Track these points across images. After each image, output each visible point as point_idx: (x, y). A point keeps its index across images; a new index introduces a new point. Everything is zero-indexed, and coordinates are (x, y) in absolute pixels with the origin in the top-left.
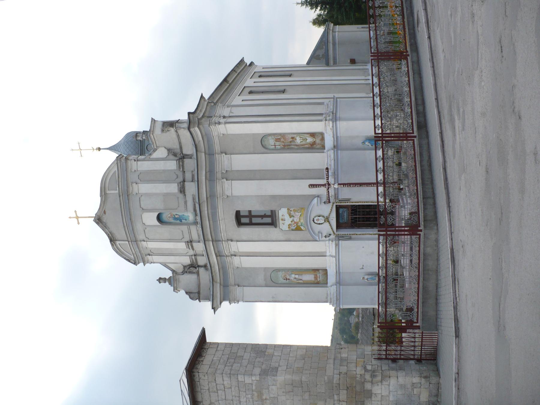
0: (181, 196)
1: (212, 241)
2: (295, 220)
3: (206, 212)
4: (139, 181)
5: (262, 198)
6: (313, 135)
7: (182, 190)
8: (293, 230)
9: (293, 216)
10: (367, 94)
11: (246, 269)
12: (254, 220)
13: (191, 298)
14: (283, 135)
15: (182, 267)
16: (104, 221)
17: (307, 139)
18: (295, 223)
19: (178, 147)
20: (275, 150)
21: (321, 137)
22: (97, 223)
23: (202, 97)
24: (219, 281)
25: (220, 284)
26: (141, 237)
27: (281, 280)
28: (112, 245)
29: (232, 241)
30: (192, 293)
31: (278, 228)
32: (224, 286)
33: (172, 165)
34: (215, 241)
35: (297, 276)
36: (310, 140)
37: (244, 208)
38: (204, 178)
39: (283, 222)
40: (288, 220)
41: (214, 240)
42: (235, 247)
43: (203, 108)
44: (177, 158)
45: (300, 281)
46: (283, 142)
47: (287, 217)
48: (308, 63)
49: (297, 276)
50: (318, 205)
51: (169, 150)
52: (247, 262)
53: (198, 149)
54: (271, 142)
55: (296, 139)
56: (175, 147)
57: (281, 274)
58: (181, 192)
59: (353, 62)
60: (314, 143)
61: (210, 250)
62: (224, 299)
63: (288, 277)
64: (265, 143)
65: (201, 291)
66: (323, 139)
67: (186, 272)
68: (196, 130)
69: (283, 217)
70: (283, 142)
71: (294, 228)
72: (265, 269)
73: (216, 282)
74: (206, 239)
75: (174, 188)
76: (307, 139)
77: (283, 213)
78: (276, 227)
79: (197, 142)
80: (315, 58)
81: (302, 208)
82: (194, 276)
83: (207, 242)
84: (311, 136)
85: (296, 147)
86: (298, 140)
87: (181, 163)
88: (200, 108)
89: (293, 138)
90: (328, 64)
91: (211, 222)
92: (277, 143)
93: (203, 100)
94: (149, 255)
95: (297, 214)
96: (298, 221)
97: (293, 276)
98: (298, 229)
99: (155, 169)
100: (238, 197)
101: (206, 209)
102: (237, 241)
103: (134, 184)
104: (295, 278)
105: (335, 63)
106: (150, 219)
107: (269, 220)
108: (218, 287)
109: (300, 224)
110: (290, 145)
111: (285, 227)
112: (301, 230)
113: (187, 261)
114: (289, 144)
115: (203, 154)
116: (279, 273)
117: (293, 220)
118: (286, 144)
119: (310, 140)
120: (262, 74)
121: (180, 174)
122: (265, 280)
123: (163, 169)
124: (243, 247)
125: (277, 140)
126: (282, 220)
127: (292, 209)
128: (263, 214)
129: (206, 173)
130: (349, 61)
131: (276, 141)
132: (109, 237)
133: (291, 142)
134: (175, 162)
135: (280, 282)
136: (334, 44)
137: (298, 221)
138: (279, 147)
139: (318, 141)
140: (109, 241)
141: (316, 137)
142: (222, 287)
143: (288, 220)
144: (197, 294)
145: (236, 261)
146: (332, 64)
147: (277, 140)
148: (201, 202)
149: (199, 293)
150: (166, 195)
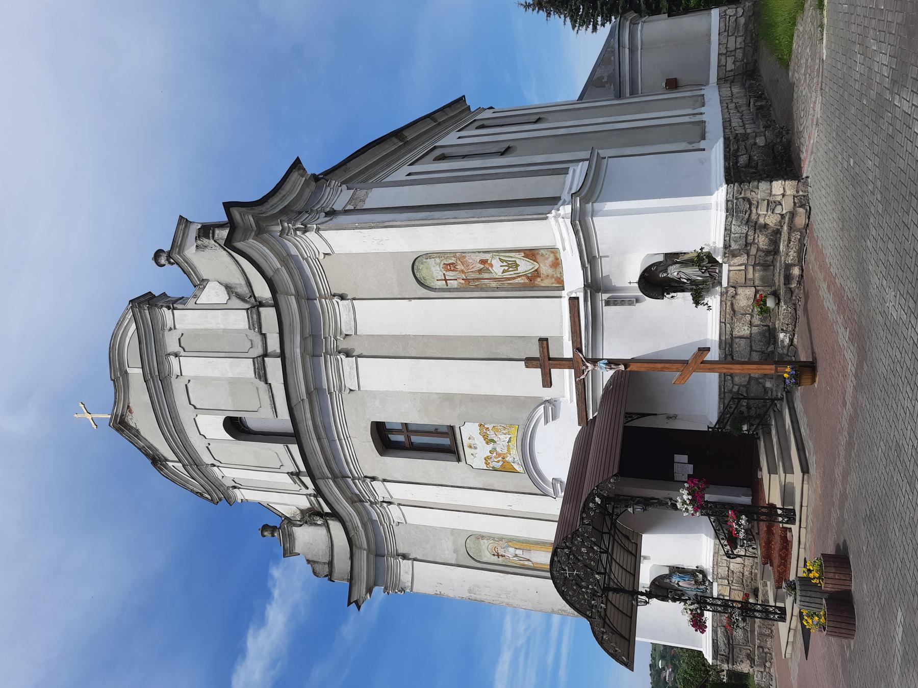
0: (262, 385)
1: (335, 478)
2: (499, 450)
3: (310, 423)
4: (182, 353)
5: (425, 399)
6: (531, 254)
7: (261, 373)
8: (495, 470)
9: (493, 441)
10: (690, 143)
11: (416, 526)
12: (416, 439)
13: (315, 573)
14: (461, 255)
15: (298, 512)
16: (133, 425)
17: (517, 265)
18: (499, 455)
19: (243, 282)
20: (446, 292)
21: (551, 258)
22: (118, 430)
23: (297, 165)
24: (365, 545)
25: (369, 551)
26: (207, 459)
27: (488, 557)
28: (160, 470)
29: (373, 479)
30: (317, 562)
31: (462, 463)
32: (377, 555)
33: (238, 319)
34: (339, 477)
35: (519, 552)
36: (525, 266)
37: (393, 416)
38: (298, 351)
39: (473, 451)
40: (484, 450)
41: (339, 475)
42: (381, 490)
43: (291, 192)
44: (247, 306)
45: (526, 563)
46: (463, 271)
47: (479, 441)
48: (581, 98)
49: (519, 552)
50: (546, 422)
51: (229, 288)
52: (415, 516)
53: (279, 287)
54: (434, 272)
55: (491, 265)
56: (237, 281)
57: (485, 543)
58: (260, 378)
59: (672, 84)
60: (536, 274)
61: (333, 494)
62: (375, 584)
63: (501, 552)
64: (423, 273)
65: (335, 561)
66: (557, 264)
67: (306, 523)
68: (252, 245)
69: (471, 442)
70: (463, 271)
71: (498, 465)
72: (453, 532)
73: (361, 548)
74: (317, 473)
75: (246, 368)
76: (517, 265)
77: (469, 433)
78: (459, 460)
79: (270, 273)
80: (594, 84)
81: (511, 425)
82: (322, 531)
83: (321, 483)
84: (526, 256)
85: (494, 284)
86: (497, 269)
87: (255, 316)
88: (282, 193)
89: (483, 262)
90: (619, 96)
91: (325, 442)
92: (450, 275)
93: (295, 175)
94: (235, 487)
95: (502, 437)
96: (505, 451)
97: (512, 550)
98: (507, 469)
99: (208, 326)
100: (373, 394)
101: (308, 415)
102: (384, 480)
103: (172, 358)
104: (516, 556)
105: (634, 92)
106: (212, 427)
107: (446, 441)
108: (362, 557)
109: (509, 459)
110: (478, 279)
111: (479, 463)
112: (515, 471)
113: (305, 503)
114: (477, 276)
115: (293, 300)
116: (482, 542)
117: (494, 449)
118: (473, 276)
119: (525, 266)
120: (486, 123)
121: (258, 339)
122: (456, 551)
123: (222, 326)
124: (398, 492)
125: (450, 267)
126: (470, 447)
127: (490, 426)
128: (433, 429)
129: (303, 338)
130: (664, 85)
131: (448, 270)
132: (147, 455)
133: (480, 271)
134: (244, 312)
135: (485, 560)
136: (632, 51)
137: (505, 451)
138: (453, 284)
139: (545, 269)
140: (149, 462)
141: (539, 258)
142: (372, 557)
143: (484, 450)
144: (326, 566)
145: (393, 510)
146: (628, 95)
147: (450, 267)
148: (294, 402)
149: (331, 564)
150: (235, 383)
